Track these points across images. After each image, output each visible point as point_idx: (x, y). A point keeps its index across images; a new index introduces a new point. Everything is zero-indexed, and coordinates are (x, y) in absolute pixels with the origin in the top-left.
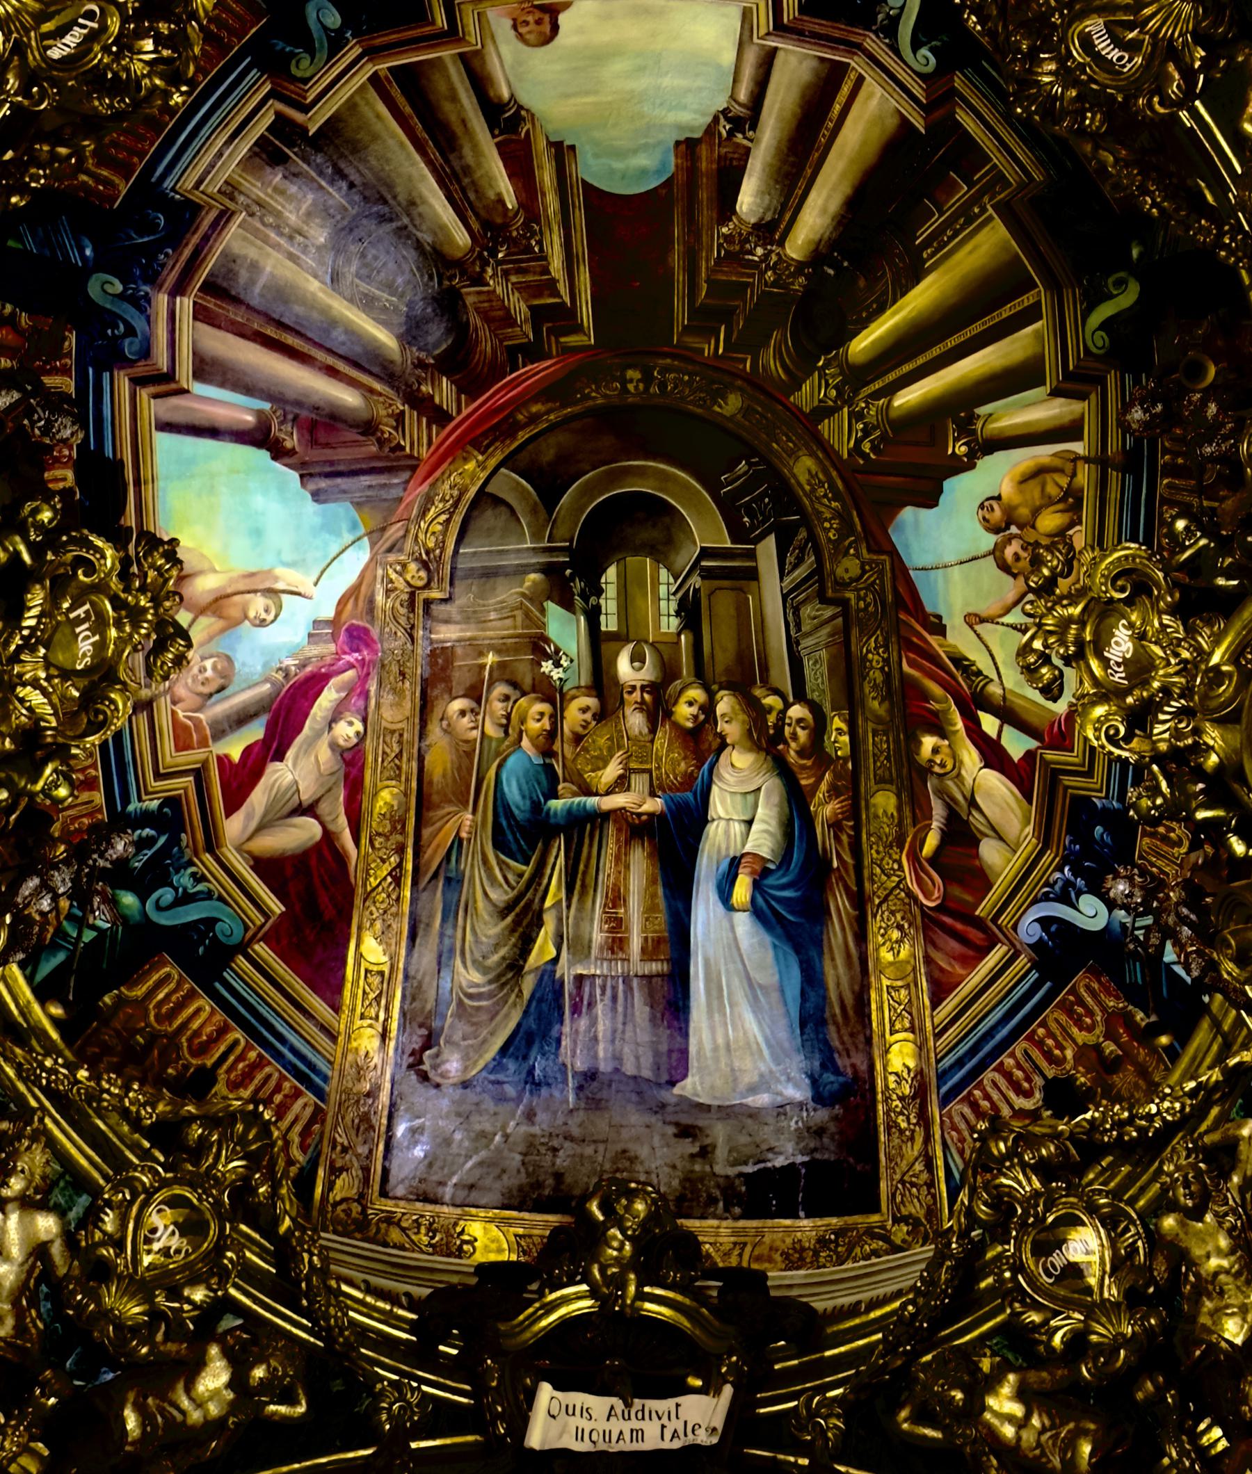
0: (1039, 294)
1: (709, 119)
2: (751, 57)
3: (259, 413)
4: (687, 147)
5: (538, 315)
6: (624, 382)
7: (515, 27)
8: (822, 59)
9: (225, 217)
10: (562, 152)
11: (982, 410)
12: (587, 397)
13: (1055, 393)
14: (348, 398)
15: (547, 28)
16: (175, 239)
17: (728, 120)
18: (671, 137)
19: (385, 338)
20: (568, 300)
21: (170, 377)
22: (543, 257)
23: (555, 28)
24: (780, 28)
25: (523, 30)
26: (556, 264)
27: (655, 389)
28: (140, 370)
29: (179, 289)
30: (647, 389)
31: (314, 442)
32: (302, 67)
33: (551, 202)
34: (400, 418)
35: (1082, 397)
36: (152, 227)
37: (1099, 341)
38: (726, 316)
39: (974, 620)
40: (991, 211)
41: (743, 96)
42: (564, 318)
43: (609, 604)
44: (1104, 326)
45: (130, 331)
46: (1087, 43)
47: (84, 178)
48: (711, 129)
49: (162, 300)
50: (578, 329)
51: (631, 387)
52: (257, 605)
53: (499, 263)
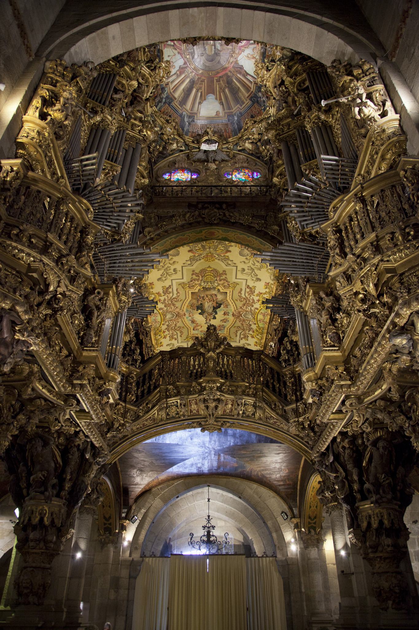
0: (172, 91)
4: (205, 100)
5: (219, 81)
9: (248, 97)
10: (216, 99)
14: (238, 75)
16: (252, 97)
19: (234, 80)
24: (196, 114)
32: (238, 112)
33: (218, 93)
37: (166, 89)
38: (201, 81)
39: (175, 55)
43: (213, 49)
46: (171, 129)
52: (249, 56)
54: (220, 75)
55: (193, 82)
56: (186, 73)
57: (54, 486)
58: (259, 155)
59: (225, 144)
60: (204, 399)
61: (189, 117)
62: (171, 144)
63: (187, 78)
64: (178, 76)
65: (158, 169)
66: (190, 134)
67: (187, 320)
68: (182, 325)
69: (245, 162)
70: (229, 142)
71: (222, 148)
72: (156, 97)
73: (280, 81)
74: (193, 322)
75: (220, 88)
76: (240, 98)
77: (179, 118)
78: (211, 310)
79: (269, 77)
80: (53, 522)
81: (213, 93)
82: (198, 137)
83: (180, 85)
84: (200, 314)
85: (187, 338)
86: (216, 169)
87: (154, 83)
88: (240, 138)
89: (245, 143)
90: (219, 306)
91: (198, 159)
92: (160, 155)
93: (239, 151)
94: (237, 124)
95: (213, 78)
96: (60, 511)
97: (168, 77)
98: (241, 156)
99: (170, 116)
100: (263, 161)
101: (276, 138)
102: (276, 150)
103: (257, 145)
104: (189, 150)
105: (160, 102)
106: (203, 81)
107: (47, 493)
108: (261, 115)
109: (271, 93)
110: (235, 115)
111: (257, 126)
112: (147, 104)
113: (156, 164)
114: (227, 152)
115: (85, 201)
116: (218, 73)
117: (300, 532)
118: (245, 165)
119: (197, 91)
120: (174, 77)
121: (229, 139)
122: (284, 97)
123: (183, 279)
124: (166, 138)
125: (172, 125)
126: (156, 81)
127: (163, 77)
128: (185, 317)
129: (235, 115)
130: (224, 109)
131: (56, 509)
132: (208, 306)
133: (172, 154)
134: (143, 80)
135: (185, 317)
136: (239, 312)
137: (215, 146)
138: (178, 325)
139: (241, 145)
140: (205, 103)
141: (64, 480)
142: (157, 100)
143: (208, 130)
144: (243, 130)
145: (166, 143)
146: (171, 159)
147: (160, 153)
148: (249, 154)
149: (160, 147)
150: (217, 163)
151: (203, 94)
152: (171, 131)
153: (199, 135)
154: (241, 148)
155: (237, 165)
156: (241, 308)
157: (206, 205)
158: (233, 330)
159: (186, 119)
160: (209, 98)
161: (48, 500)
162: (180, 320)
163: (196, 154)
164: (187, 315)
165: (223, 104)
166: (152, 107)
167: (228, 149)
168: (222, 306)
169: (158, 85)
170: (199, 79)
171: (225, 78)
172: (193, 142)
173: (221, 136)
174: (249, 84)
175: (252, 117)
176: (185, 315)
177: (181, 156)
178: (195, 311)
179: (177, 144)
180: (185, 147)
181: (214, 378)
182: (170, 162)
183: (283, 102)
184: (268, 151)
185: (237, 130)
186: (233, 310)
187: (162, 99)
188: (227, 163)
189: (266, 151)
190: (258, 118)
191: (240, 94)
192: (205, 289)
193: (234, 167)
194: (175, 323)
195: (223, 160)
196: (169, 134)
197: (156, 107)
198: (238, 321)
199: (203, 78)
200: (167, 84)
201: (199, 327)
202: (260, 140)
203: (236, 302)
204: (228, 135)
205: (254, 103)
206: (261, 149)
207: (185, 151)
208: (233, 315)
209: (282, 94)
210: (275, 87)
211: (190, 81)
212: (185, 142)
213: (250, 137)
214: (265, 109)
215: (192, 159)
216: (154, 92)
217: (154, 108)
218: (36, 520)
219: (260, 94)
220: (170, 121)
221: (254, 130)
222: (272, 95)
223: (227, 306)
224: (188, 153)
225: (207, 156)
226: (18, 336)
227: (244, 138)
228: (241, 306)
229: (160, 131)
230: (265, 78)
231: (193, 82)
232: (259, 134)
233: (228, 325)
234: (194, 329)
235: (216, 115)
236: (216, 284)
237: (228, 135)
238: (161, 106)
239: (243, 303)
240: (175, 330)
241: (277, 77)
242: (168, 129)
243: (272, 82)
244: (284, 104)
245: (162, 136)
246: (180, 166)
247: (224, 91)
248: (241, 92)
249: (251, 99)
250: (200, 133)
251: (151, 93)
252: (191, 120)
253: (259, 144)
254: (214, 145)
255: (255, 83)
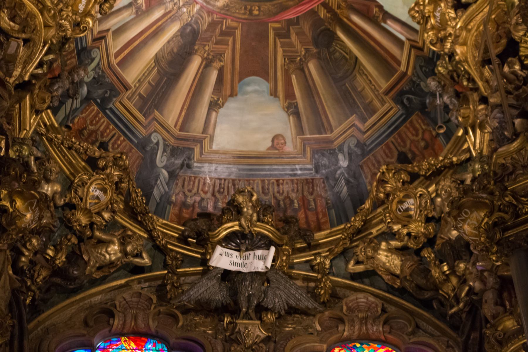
0: (114, 62)
1: (226, 104)
2: (210, 131)
3: (385, 22)
4: (233, 94)
5: (288, 36)
6: (259, 10)
7: (285, 143)
8: (187, 132)
9: (387, 92)
10: (274, 93)
11: (133, 16)
12: (273, 5)
13: (108, 30)
14: (356, 19)
15: (276, 141)
16: (402, 93)
17: (219, 105)
18: (239, 96)
20: (277, 39)
21: (412, 47)
22: (284, 57)
23: (273, 141)
24: (200, 141)
25: (283, 141)
26: (280, 51)
27: (249, 7)
28: (420, 53)
29: (405, 74)
30: (251, 7)
31: (369, 9)
32: (354, 142)
34: (339, 7)
35: (99, 32)
36: (408, 99)
37: (95, 53)
38: (222, 33)
40: (133, 86)
41: (214, 114)
42: (279, 34)
44: (93, 60)
45: (421, 67)
46: (104, 191)
47: (424, 127)
48: (225, 100)
49: (409, 73)
50: (274, 29)
51: (257, 8)
53: (300, 56)
54: (290, 15)
55: (195, 33)
56: (170, 6)
58: (427, 295)
59: (301, 250)
61: (174, 152)
62: (101, 242)
63: (173, 20)
64: (140, 14)
65: (47, 331)
66: (172, 211)
69: (376, 319)
70: (318, 246)
71: (292, 266)
72: (56, 79)
73: (504, 41)
75: (290, 59)
76: (361, 94)
77: (136, 153)
79: (465, 27)
81: (264, 73)
82: (202, 224)
83: (145, 43)
86: (267, 340)
87: (52, 32)
88: (359, 231)
89: (376, 249)
91: (198, 302)
92: (58, 280)
93: (354, 277)
94: (348, 182)
95: (266, 24)
97: (105, 16)
98: (362, 298)
99: (103, 146)
100: (442, 316)
101: (490, 238)
102: (491, 281)
103: (422, 259)
104: (165, 266)
105: (67, 95)
106: (229, 32)
108: (436, 156)
109: (471, 80)
110: (341, 149)
111: (420, 190)
112: (20, 100)
113: (40, 312)
114: (307, 279)
116: (284, 8)
118: (377, 329)
119: (207, 64)
120: (126, 16)
121: (318, 235)
122: (517, 98)
124: (84, 221)
125: (109, 176)
126: (61, 26)
127: (87, 13)
129: (341, 149)
130: (300, 130)
133: (103, 280)
134: (12, 19)
137: (264, 258)
139: (361, 257)
140: (231, 105)
142: (59, 89)
143: (240, 199)
144: (367, 205)
145: (81, 240)
146: (98, 298)
147: (57, 272)
148: (390, 289)
149: (57, 251)
150: (270, 317)
151: (228, 76)
152: (104, 198)
153: (205, 215)
154: (360, 268)
159: (161, 159)
160: (249, 89)
163: (193, 284)
165: (297, 114)
166: (38, 112)
167: (312, 269)
169: (65, 40)
170: (213, 25)
171: (306, 27)
172: (183, 240)
173: (287, 221)
174: (394, 50)
175: (403, 159)
177: (136, 287)
179: (123, 244)
180: (152, 258)
182: (91, 307)
183: (515, 112)
184: (463, 281)
185: (348, 204)
187: (77, 85)
188: (307, 321)
189: (454, 281)
190: (425, 165)
191: (360, 82)
193: (333, 338)
195: (292, 311)
196: (94, 209)
197: (55, 113)
199: (230, 22)
200: (101, 38)
202: (431, 242)
204: (312, 217)
205: (408, 112)
206: (435, 273)
207: (150, 269)
209: (510, 87)
210: (486, 62)
211: (182, 32)
212: (152, 238)
213: (396, 228)
214: (448, 135)
215: (175, 302)
216: (51, 62)
217: (48, 117)
219: (432, 84)
220: (101, 163)
221: (410, 203)
222: (476, 89)
224: (163, 277)
225: (234, 293)
227: (374, 231)
229: (62, 194)
230: (450, 30)
231: (195, 33)
232: (428, 220)
235: (273, 147)
237: (312, 217)
238: (74, 111)
241: (491, 28)
242: (94, 191)
243: (476, 46)
244: (517, 121)
245: (68, 214)
246: (131, 324)
247: (302, 69)
248: (363, 72)
249: (398, 99)
250: (210, 208)
251: (40, 65)
252: (179, 162)
253: (427, 254)
254: (259, 252)
255: (416, 47)
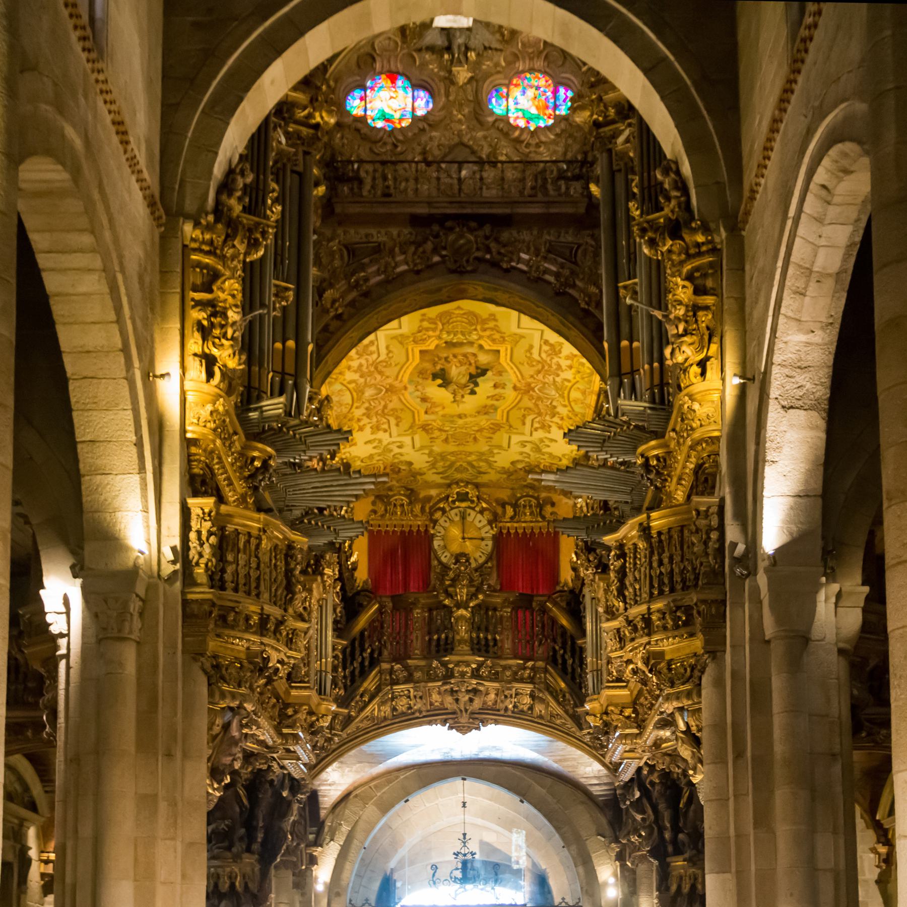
57: (241, 839)
60: (452, 689)
67: (411, 398)
68: (400, 406)
74: (424, 400)
78: (464, 380)
80: (246, 887)
84: (440, 386)
85: (411, 427)
90: (483, 372)
96: (253, 870)
107: (234, 850)
115: (260, 445)
117: (623, 866)
123: (400, 328)
128: (407, 394)
131: (248, 870)
132: (456, 372)
135: (407, 394)
136: (529, 384)
138: (391, 406)
141: (255, 829)
155: (520, 66)
156: (532, 376)
157: (449, 224)
158: (516, 415)
161: (237, 858)
162: (395, 398)
164: (411, 388)
168: (489, 373)
176: (406, 388)
178: (430, 381)
181: (467, 658)
186: (514, 379)
192: (450, 344)
194: (383, 403)
198: (526, 398)
201: (437, 410)
203: (521, 367)
208: (515, 388)
218: (225, 887)
223: (500, 373)
226: (245, 731)
228: (532, 373)
233: (503, 406)
234: (426, 413)
236: (475, 337)
239: (536, 368)
240: (384, 414)
